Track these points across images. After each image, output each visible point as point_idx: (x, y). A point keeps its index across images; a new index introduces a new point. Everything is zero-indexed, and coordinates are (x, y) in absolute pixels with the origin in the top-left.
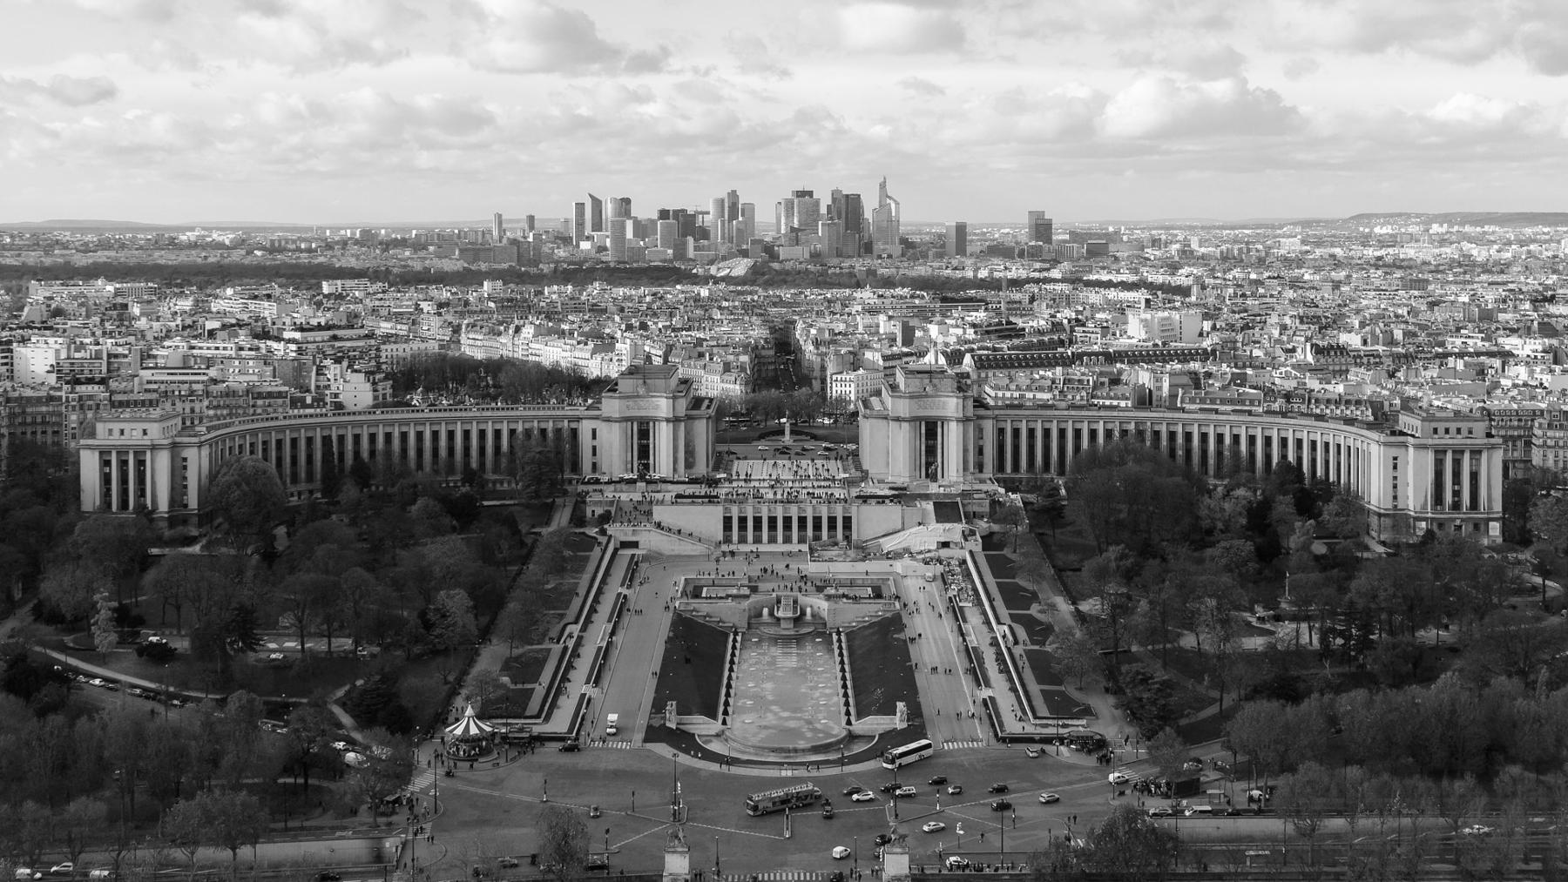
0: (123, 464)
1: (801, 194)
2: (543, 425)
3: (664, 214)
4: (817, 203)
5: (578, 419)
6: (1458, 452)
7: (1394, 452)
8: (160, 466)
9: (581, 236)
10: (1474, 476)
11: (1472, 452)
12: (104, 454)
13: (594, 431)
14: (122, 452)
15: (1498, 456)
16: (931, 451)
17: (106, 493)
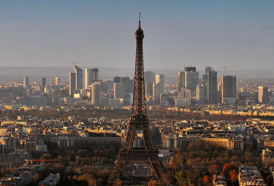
0: (63, 142)
1: (189, 69)
2: (116, 140)
3: (117, 79)
4: (197, 74)
5: (121, 139)
6: (237, 142)
7: (230, 142)
8: (68, 143)
9: (74, 91)
10: (240, 145)
11: (239, 142)
12: (61, 141)
13: (123, 141)
14: (63, 141)
15: (243, 143)
16: (172, 144)
17: (61, 146)
